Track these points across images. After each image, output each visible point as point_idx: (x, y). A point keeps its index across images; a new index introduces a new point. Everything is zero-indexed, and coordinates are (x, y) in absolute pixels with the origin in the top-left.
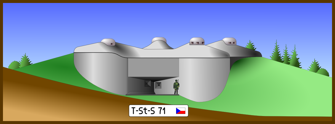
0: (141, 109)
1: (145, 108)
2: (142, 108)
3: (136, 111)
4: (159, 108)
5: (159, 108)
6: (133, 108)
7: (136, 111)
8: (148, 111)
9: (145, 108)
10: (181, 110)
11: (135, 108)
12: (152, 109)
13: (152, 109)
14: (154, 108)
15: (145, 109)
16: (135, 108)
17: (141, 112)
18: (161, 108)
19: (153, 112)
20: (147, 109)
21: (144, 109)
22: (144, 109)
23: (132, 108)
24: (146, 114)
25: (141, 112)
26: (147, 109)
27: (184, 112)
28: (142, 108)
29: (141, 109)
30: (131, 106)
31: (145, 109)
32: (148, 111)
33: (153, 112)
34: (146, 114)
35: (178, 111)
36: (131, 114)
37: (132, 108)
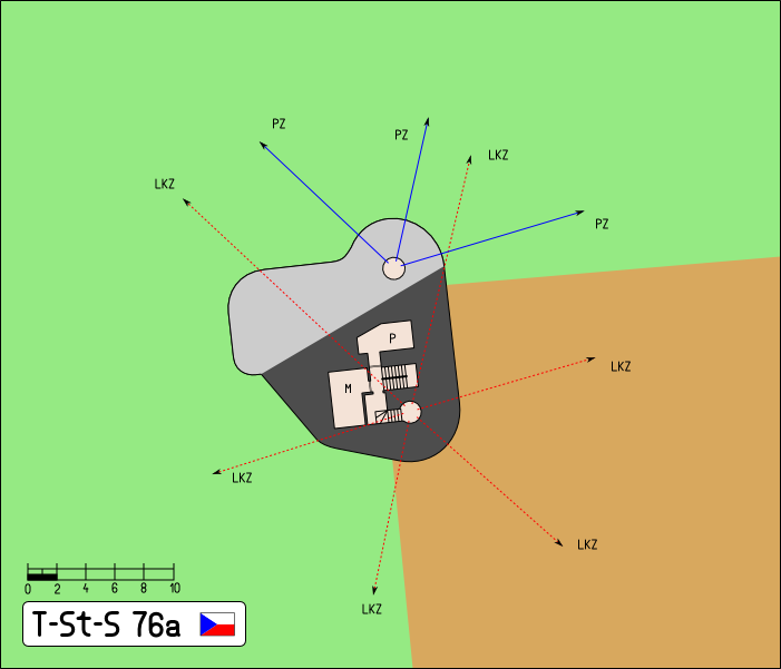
0: (66, 618)
1: (84, 613)
2: (72, 613)
3: (52, 624)
4: (135, 613)
5: (135, 613)
6: (40, 614)
7: (52, 624)
8: (96, 624)
9: (84, 613)
10: (218, 620)
11: (44, 613)
12: (111, 618)
13: (111, 618)
14: (117, 613)
15: (83, 618)
16: (44, 613)
17: (69, 630)
18: (144, 613)
19: (113, 630)
20: (89, 618)
21: (78, 618)
22: (78, 618)
23: (35, 613)
24: (89, 635)
25: (69, 630)
26: (89, 618)
27: (228, 630)
28: (72, 613)
29: (66, 618)
30: (30, 608)
31: (83, 618)
32: (96, 624)
33: (113, 630)
34: (89, 635)
35: (207, 626)
36: (31, 636)
37: (35, 613)
